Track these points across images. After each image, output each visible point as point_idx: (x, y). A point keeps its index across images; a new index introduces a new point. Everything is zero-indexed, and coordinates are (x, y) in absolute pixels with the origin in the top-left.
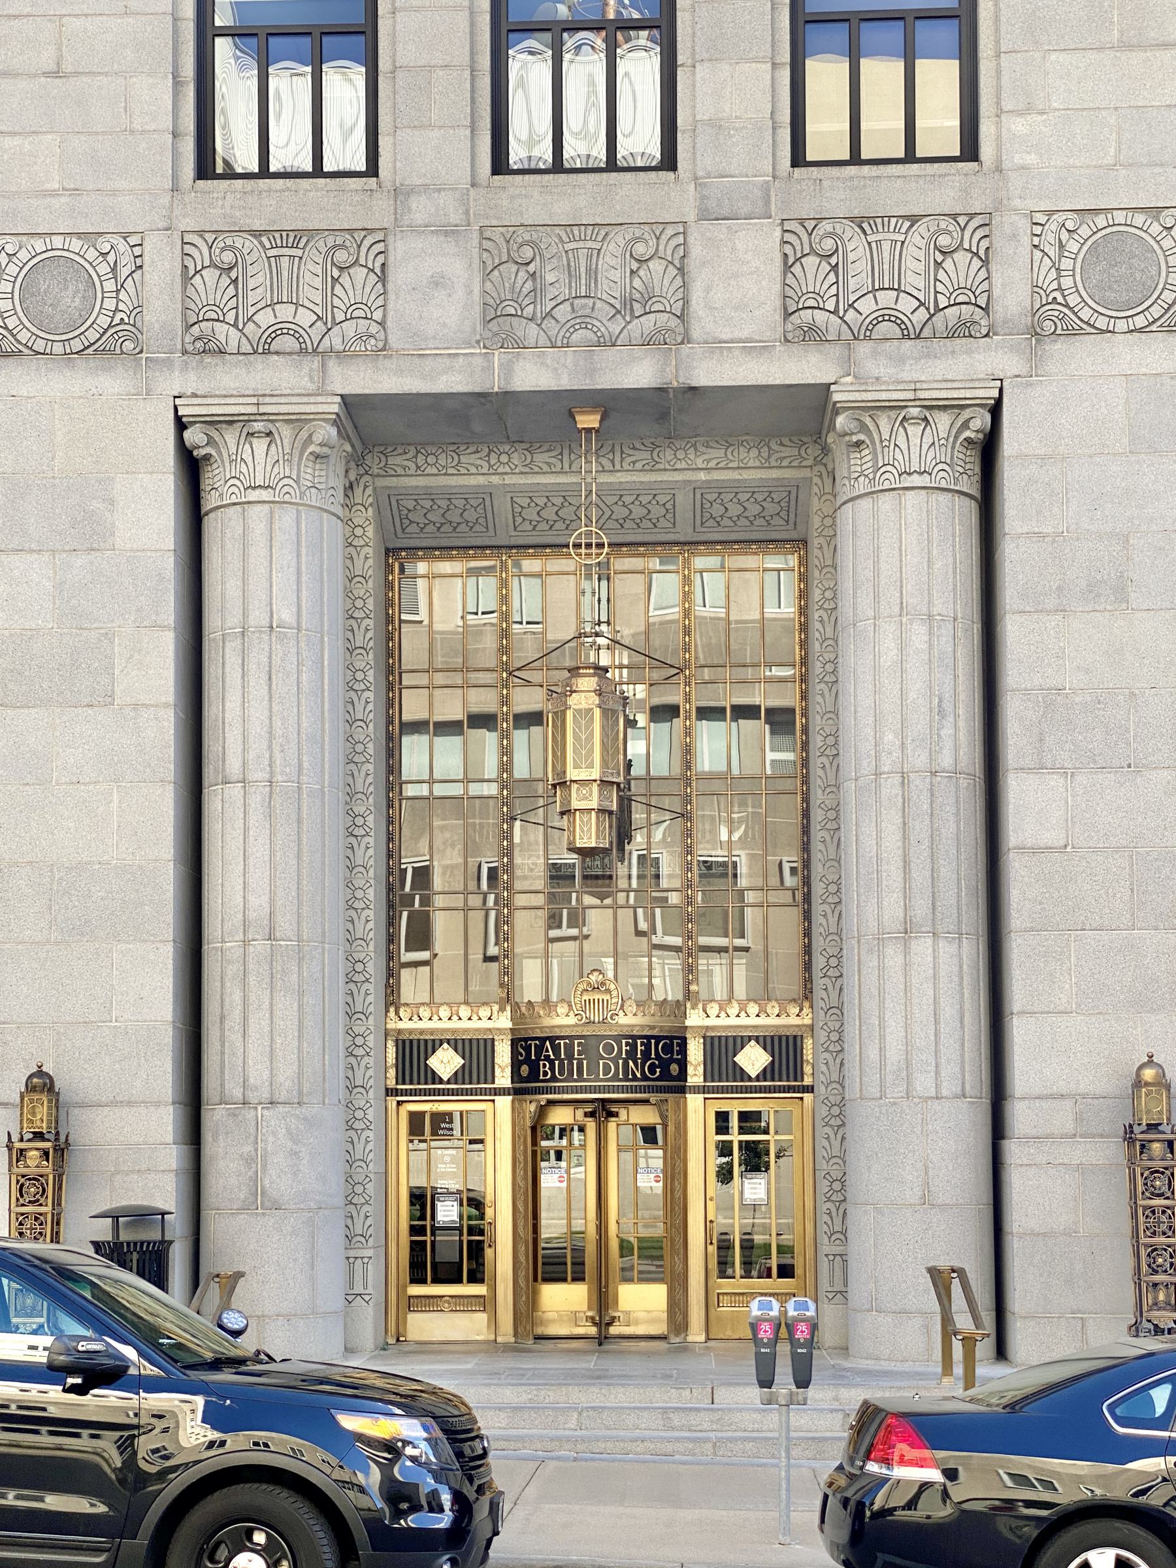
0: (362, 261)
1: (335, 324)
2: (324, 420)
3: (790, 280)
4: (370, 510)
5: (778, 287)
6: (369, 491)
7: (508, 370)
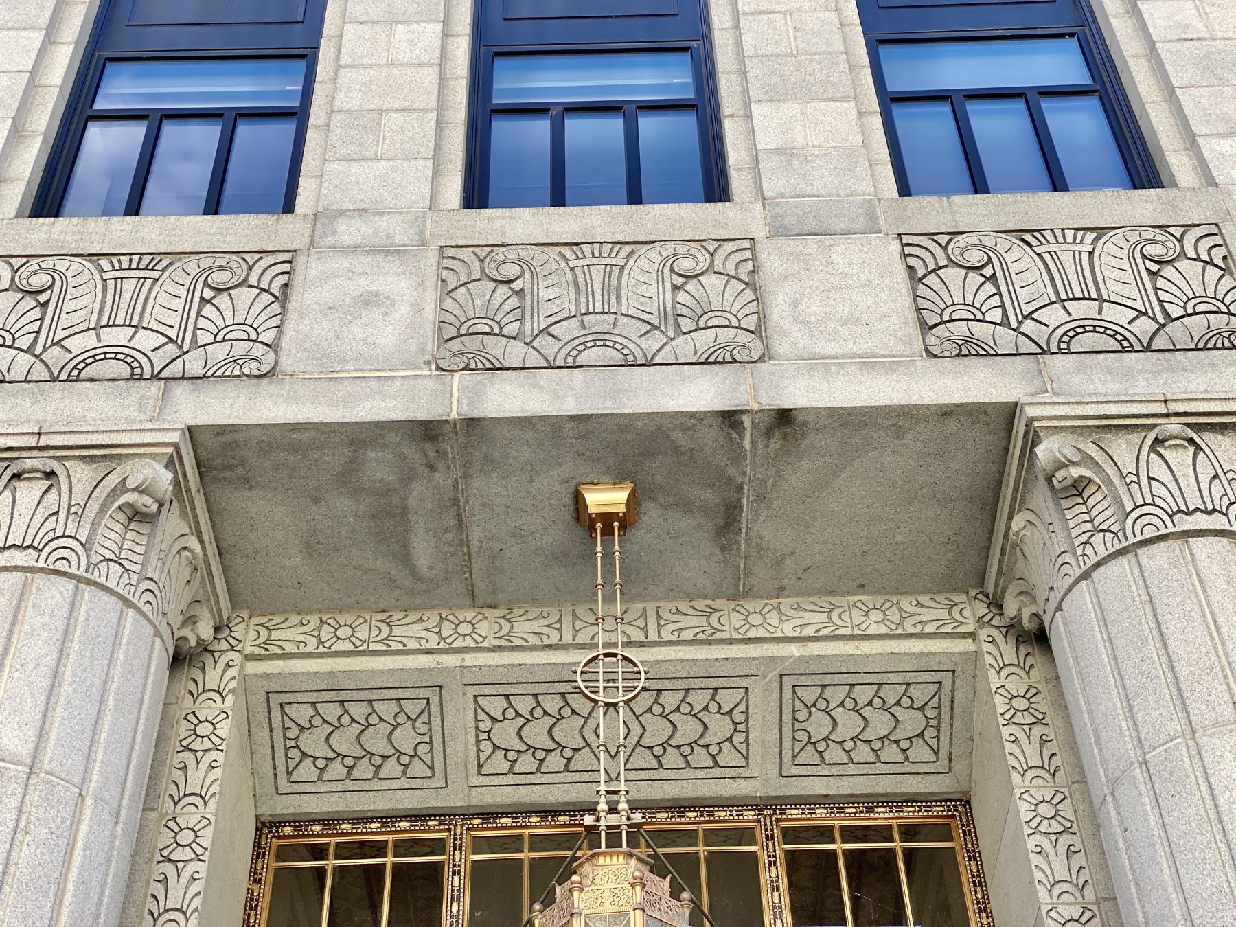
0: (253, 280)
1: (195, 344)
2: (154, 456)
3: (922, 290)
4: (230, 699)
5: (907, 299)
6: (232, 672)
7: (477, 394)
